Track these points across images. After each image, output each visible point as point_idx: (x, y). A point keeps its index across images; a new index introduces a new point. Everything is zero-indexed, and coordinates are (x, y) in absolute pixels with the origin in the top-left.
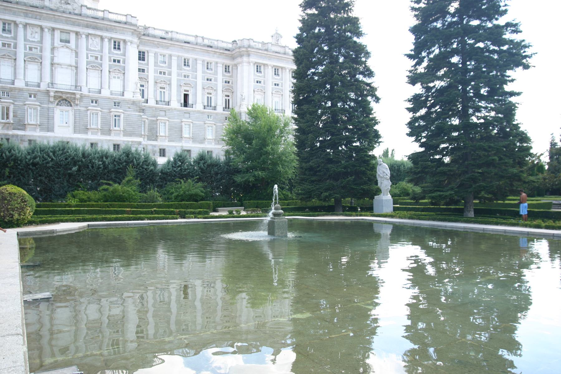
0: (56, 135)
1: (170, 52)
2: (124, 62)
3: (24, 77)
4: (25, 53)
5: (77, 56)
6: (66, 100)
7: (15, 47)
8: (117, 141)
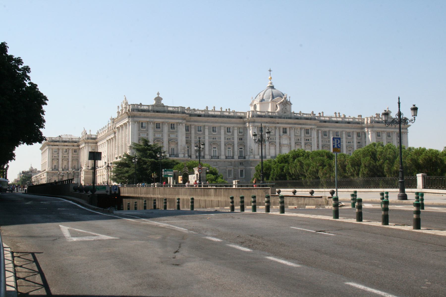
2: (311, 141)
5: (290, 140)
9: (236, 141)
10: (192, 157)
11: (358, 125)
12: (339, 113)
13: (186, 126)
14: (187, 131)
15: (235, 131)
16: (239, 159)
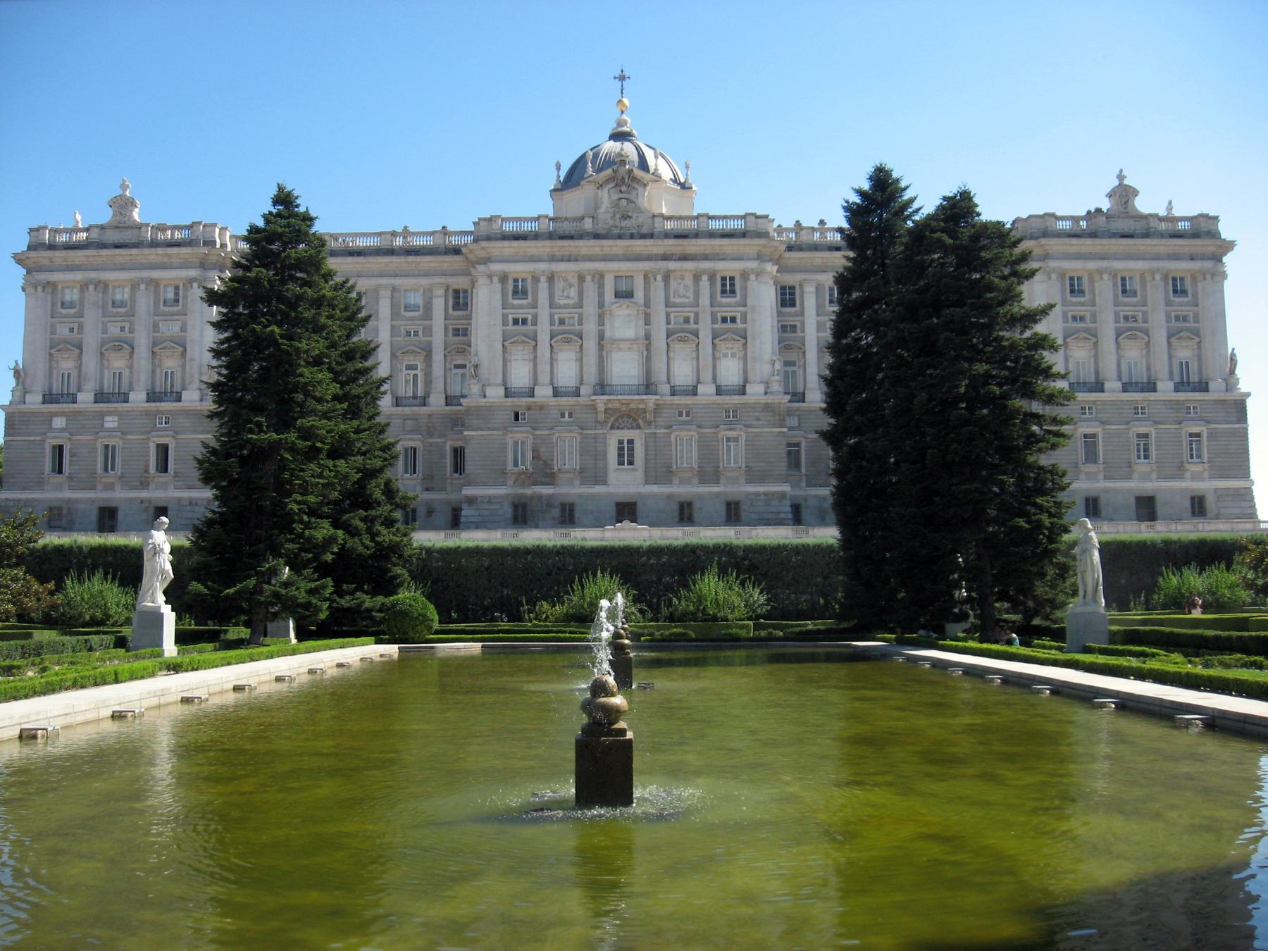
0: (611, 490)
2: (744, 321)
3: (552, 380)
4: (551, 331)
5: (647, 322)
6: (629, 416)
7: (535, 323)
9: (438, 339)
15: (434, 300)
16: (447, 405)
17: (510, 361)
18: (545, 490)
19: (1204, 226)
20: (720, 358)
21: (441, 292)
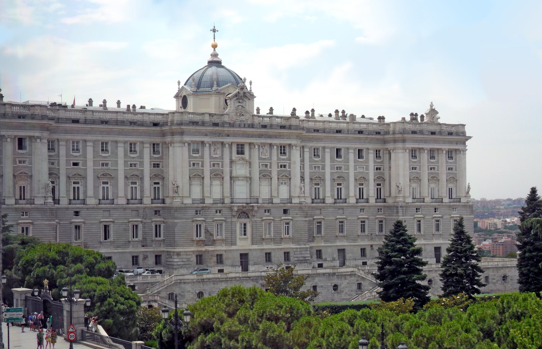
1: (323, 145)
2: (290, 168)
7: (202, 166)
8: (287, 248)
10: (61, 203)
11: (378, 136)
12: (343, 112)
13: (49, 142)
14: (50, 150)
15: (145, 149)
16: (152, 203)
17: (192, 185)
18: (210, 248)
19: (461, 129)
20: (280, 185)
21: (148, 145)
